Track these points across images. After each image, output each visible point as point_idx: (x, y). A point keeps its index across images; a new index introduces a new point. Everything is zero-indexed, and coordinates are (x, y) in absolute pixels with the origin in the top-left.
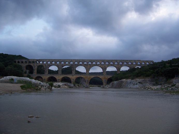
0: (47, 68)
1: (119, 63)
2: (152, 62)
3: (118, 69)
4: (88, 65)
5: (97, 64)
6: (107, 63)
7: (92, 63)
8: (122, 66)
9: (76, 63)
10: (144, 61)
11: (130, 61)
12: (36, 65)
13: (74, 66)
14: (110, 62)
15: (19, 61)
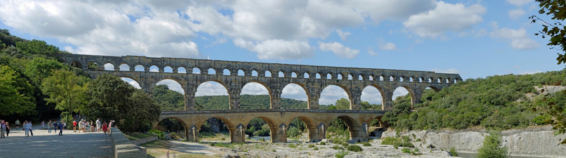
0: (192, 88)
1: (389, 77)
2: (458, 78)
3: (387, 95)
4: (317, 81)
5: (338, 81)
6: (361, 78)
7: (323, 74)
8: (395, 86)
9: (281, 75)
10: (441, 76)
11: (412, 74)
12: (152, 77)
13: (279, 85)
14: (369, 73)
15: (79, 60)
